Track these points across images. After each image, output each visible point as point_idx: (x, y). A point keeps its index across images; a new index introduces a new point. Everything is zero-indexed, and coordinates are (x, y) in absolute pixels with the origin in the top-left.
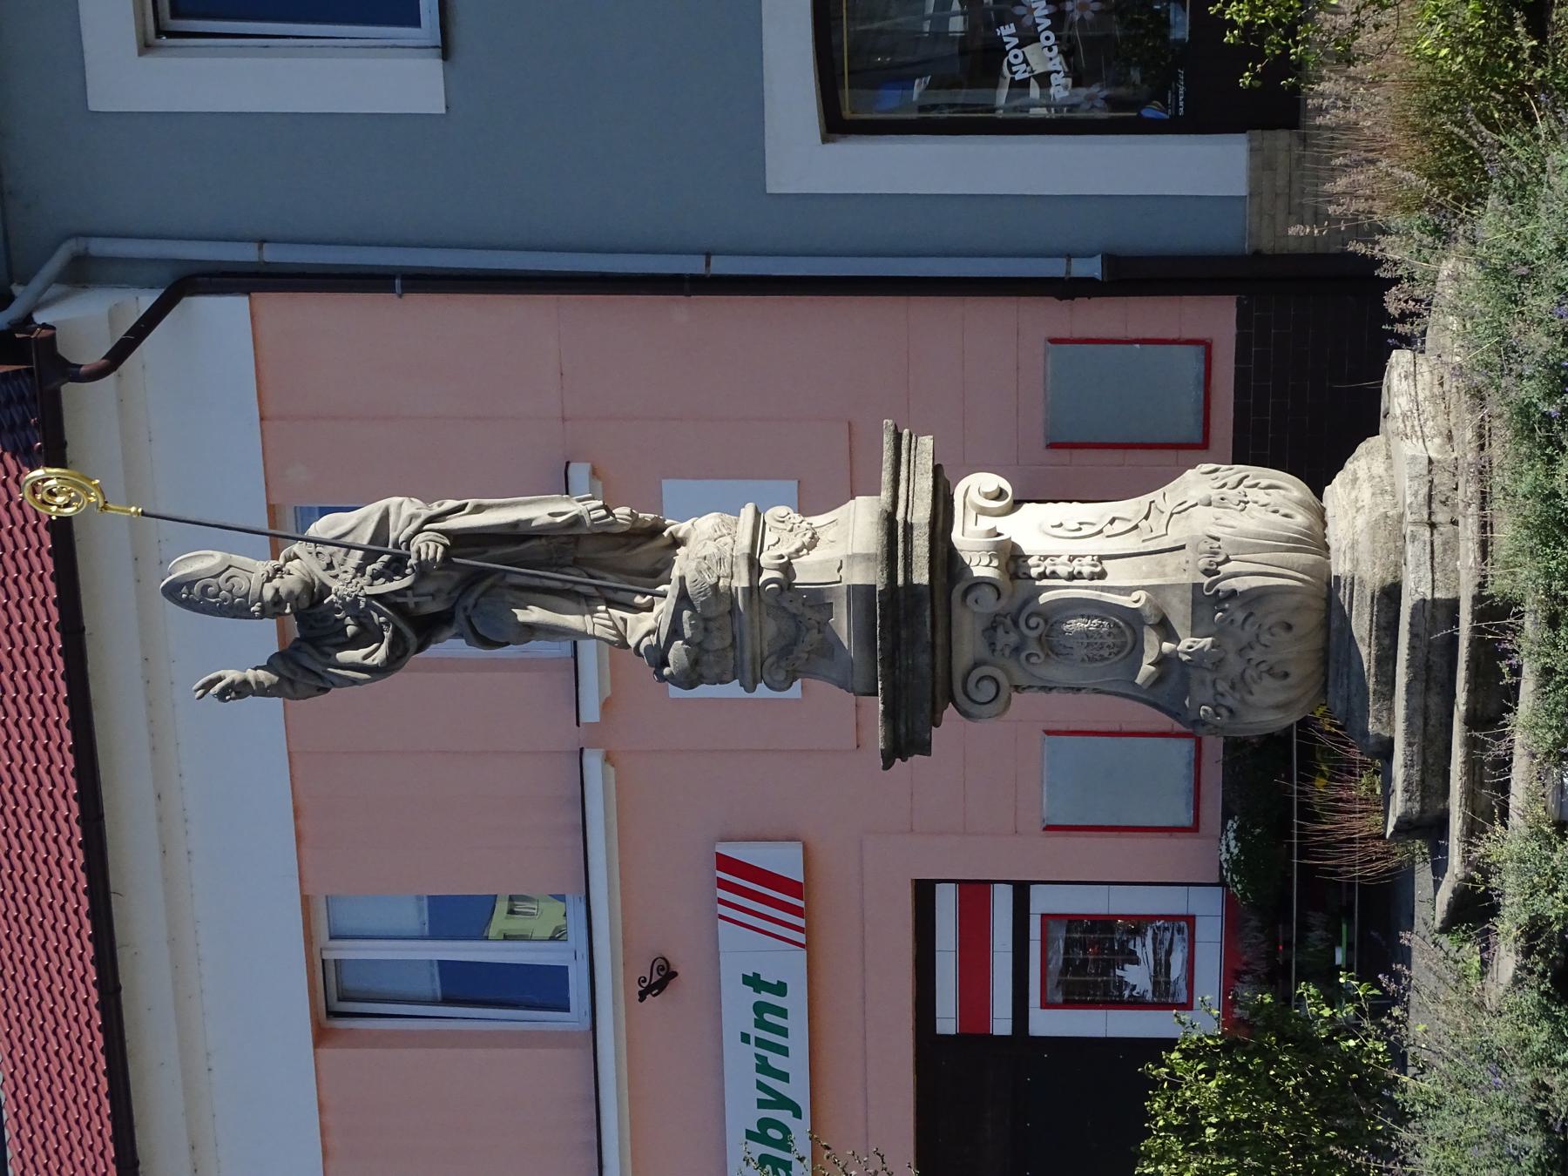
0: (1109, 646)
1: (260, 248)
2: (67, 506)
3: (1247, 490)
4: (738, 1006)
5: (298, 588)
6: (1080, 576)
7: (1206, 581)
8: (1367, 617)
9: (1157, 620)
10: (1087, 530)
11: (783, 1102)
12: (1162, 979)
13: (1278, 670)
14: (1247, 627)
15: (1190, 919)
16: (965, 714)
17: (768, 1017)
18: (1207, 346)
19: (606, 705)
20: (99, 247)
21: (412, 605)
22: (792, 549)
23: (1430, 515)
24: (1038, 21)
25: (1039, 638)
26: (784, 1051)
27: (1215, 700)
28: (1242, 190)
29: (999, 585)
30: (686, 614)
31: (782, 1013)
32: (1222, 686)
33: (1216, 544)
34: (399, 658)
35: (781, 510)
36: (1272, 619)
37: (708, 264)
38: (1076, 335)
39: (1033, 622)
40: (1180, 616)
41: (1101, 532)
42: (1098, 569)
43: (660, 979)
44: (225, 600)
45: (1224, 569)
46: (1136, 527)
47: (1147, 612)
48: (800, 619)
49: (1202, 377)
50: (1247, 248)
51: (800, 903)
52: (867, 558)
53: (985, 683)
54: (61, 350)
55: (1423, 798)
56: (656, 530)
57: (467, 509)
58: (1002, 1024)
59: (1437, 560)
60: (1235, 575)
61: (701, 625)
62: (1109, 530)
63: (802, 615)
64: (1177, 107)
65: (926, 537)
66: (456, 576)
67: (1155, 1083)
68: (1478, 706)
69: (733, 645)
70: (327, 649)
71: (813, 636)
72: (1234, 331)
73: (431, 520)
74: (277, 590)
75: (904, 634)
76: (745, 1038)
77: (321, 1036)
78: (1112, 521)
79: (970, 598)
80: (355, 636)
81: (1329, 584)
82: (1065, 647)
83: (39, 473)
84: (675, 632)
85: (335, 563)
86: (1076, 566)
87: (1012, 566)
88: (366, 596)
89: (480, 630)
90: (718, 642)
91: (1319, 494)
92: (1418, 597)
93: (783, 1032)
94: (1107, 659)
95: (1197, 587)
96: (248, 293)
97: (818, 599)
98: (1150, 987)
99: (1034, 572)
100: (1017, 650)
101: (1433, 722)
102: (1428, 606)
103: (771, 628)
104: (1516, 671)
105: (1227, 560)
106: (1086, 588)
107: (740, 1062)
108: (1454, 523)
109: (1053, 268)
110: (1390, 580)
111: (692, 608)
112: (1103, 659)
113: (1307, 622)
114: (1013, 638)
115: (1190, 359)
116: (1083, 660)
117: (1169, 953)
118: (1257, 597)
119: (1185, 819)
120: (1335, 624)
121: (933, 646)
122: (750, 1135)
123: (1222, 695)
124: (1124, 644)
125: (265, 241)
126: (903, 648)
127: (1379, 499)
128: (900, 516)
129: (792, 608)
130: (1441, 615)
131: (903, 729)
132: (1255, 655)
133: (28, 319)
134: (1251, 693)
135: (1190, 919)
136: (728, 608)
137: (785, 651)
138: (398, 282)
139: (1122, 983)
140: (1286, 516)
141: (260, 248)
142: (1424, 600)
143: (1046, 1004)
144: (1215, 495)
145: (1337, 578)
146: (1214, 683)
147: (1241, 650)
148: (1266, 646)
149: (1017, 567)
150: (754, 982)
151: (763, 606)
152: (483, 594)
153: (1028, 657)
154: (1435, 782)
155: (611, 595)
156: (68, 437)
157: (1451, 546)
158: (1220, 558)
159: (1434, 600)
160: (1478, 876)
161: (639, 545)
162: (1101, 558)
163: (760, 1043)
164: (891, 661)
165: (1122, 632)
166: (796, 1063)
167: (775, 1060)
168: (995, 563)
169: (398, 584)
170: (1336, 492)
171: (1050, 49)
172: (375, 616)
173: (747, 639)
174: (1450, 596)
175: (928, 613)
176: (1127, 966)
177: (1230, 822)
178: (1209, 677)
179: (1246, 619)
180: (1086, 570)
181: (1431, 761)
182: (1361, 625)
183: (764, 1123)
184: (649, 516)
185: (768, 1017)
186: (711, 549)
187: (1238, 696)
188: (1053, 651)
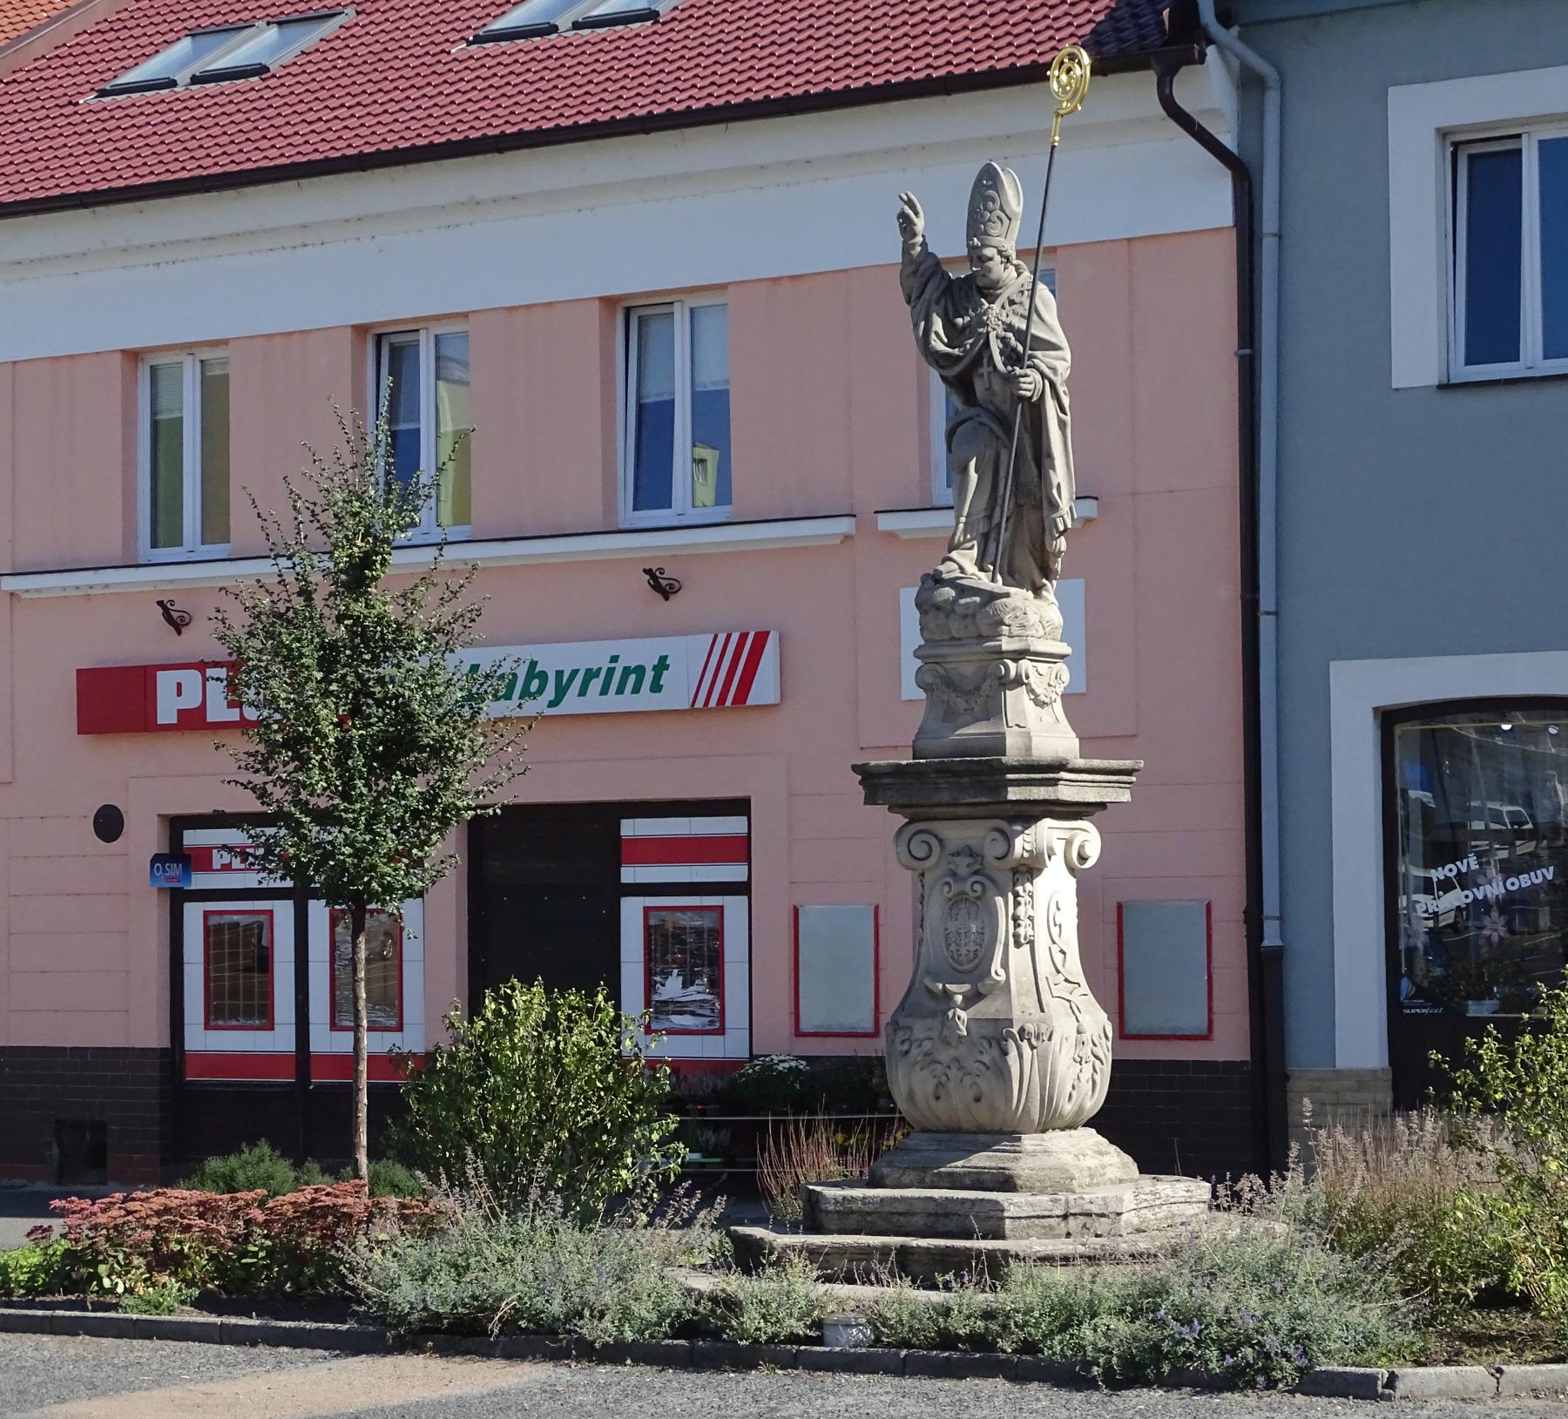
1: (1274, 235)
2: (1059, 82)
3: (1090, 1064)
4: (641, 653)
5: (993, 276)
6: (1017, 925)
7: (1015, 1031)
8: (987, 1164)
9: (981, 991)
10: (1055, 931)
11: (561, 691)
12: (670, 1008)
13: (942, 1092)
14: (977, 1064)
15: (721, 1031)
16: (900, 832)
17: (632, 678)
18: (1207, 1037)
19: (891, 535)
20: (1272, 100)
21: (981, 371)
22: (1034, 686)
23: (1074, 1215)
25: (963, 893)
26: (604, 691)
28: (1340, 1064)
29: (1009, 858)
30: (978, 599)
31: (636, 690)
32: (927, 1045)
33: (1045, 1038)
34: (937, 363)
35: (1066, 677)
36: (984, 1086)
37: (1268, 613)
38: (1214, 926)
39: (978, 887)
40: (985, 1009)
41: (1054, 942)
42: (1022, 941)
43: (662, 586)
44: (982, 216)
45: (1025, 1045)
46: (1058, 972)
47: (988, 982)
49: (1179, 1033)
50: (1292, 1068)
51: (728, 703)
52: (1029, 749)
53: (925, 847)
54: (1184, 69)
55: (838, 1212)
56: (1047, 572)
57: (1061, 415)
58: (629, 874)
59: (1037, 1221)
60: (1021, 1056)
61: (970, 611)
62: (1055, 949)
64: (1411, 1008)
65: (1047, 797)
66: (1006, 407)
67: (591, 995)
69: (953, 638)
70: (943, 300)
71: (961, 704)
72: (1221, 1059)
73: (1053, 385)
74: (991, 259)
75: (966, 780)
76: (614, 659)
77: (609, 302)
78: (1062, 952)
79: (996, 835)
80: (954, 325)
81: (1014, 1132)
83: (1086, 59)
84: (964, 591)
85: (1014, 307)
86: (1024, 922)
87: (1023, 869)
88: (988, 333)
89: (960, 429)
90: (956, 627)
91: (1087, 1124)
92: (1006, 1205)
93: (620, 691)
95: (1010, 1022)
96: (1238, 223)
97: (994, 710)
98: (663, 998)
99: (1019, 889)
100: (954, 874)
101: (902, 1219)
102: (999, 1214)
103: (968, 670)
104: (947, 1287)
105: (1032, 1047)
106: (1007, 931)
107: (594, 655)
108: (1068, 1235)
109: (1270, 906)
110: (1019, 1182)
111: (984, 604)
112: (948, 946)
113: (982, 1115)
114: (963, 870)
115: (1197, 1022)
117: (693, 1013)
118: (1003, 1074)
119: (805, 1026)
120: (982, 1138)
121: (956, 805)
122: (533, 664)
123: (920, 1045)
124: (961, 964)
125: (1280, 238)
127: (1086, 1173)
128: (1064, 775)
129: (985, 686)
130: (991, 1224)
131: (885, 781)
132: (953, 1072)
133: (1210, 41)
134: (922, 1069)
135: (721, 1031)
136: (984, 634)
137: (949, 683)
138: (1247, 351)
139: (666, 975)
140: (1070, 1096)
141: (1274, 235)
142: (1003, 1211)
143: (647, 910)
144: (1086, 1037)
145: (1019, 1139)
147: (958, 1061)
149: (1023, 873)
150: (662, 665)
152: (991, 430)
153: (948, 883)
154: (852, 1221)
155: (993, 536)
156: (1111, 77)
157: (1049, 1233)
158: (1034, 1041)
159: (1003, 1218)
160: (774, 1258)
161: (1034, 559)
162: (1031, 943)
163: (611, 671)
164: (944, 770)
165: (970, 961)
166: (594, 702)
167: (596, 684)
168: (1026, 855)
169: (998, 360)
170: (1091, 1137)
172: (971, 341)
173: (960, 650)
174: (1007, 1232)
175: (984, 800)
176: (681, 978)
177: (804, 1063)
178: (935, 1034)
179: (984, 1064)
180: (1021, 931)
181: (869, 1218)
182: (982, 1160)
183: (543, 676)
184: (1059, 567)
185: (632, 678)
186: (1033, 618)
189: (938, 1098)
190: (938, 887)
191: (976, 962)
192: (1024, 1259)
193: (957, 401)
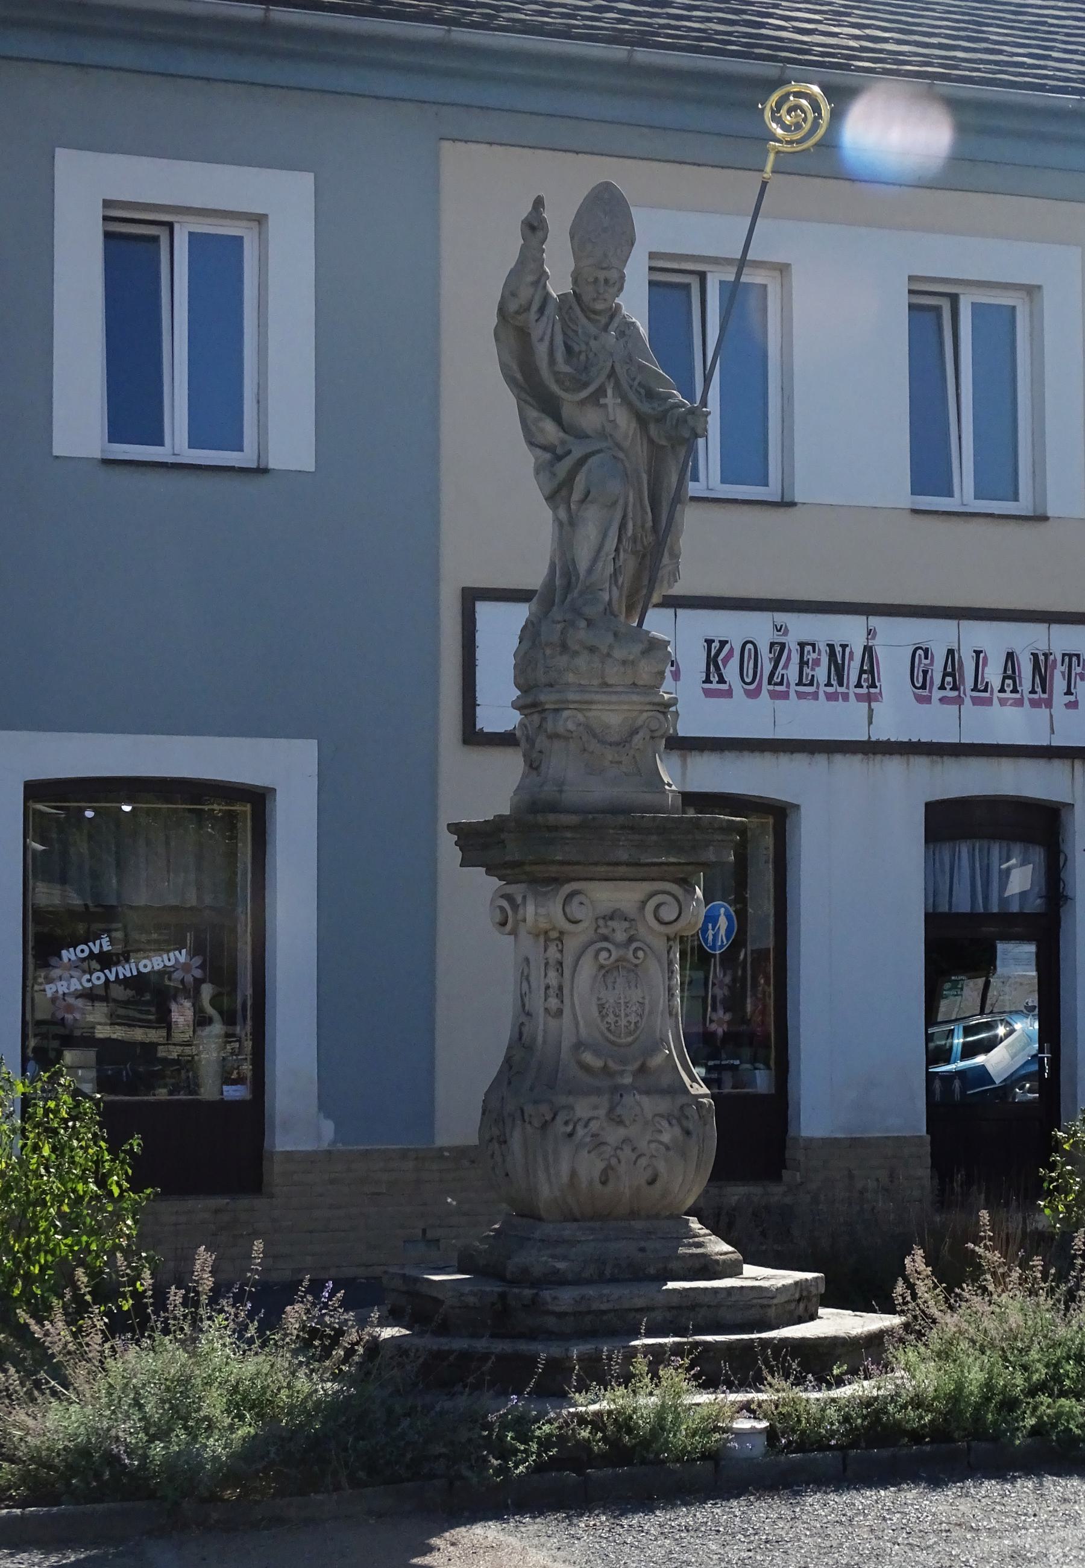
0: (617, 1022)
14: (653, 1146)
24: (114, 970)
27: (579, 1120)
36: (661, 1166)
48: (627, 745)
63: (631, 748)
68: (711, 1354)
69: (606, 685)
75: (654, 838)
82: (615, 982)
89: (591, 461)
94: (602, 1021)
112: (603, 1017)
116: (599, 999)
123: (586, 1126)
126: (637, 837)
129: (637, 739)
131: (569, 835)
132: (627, 1150)
134: (589, 1152)
146: (597, 1118)
148: (635, 1163)
151: (636, 713)
153: (636, 950)
165: (630, 1034)
171: (89, 981)
173: (614, 698)
175: (672, 860)
178: (602, 1112)
179: (661, 1143)
181: (605, 1318)
187: (588, 1139)
188: (607, 972)
189: (604, 1183)
190: (591, 951)
191: (638, 1032)
192: (103, 1369)
193: (550, 430)
